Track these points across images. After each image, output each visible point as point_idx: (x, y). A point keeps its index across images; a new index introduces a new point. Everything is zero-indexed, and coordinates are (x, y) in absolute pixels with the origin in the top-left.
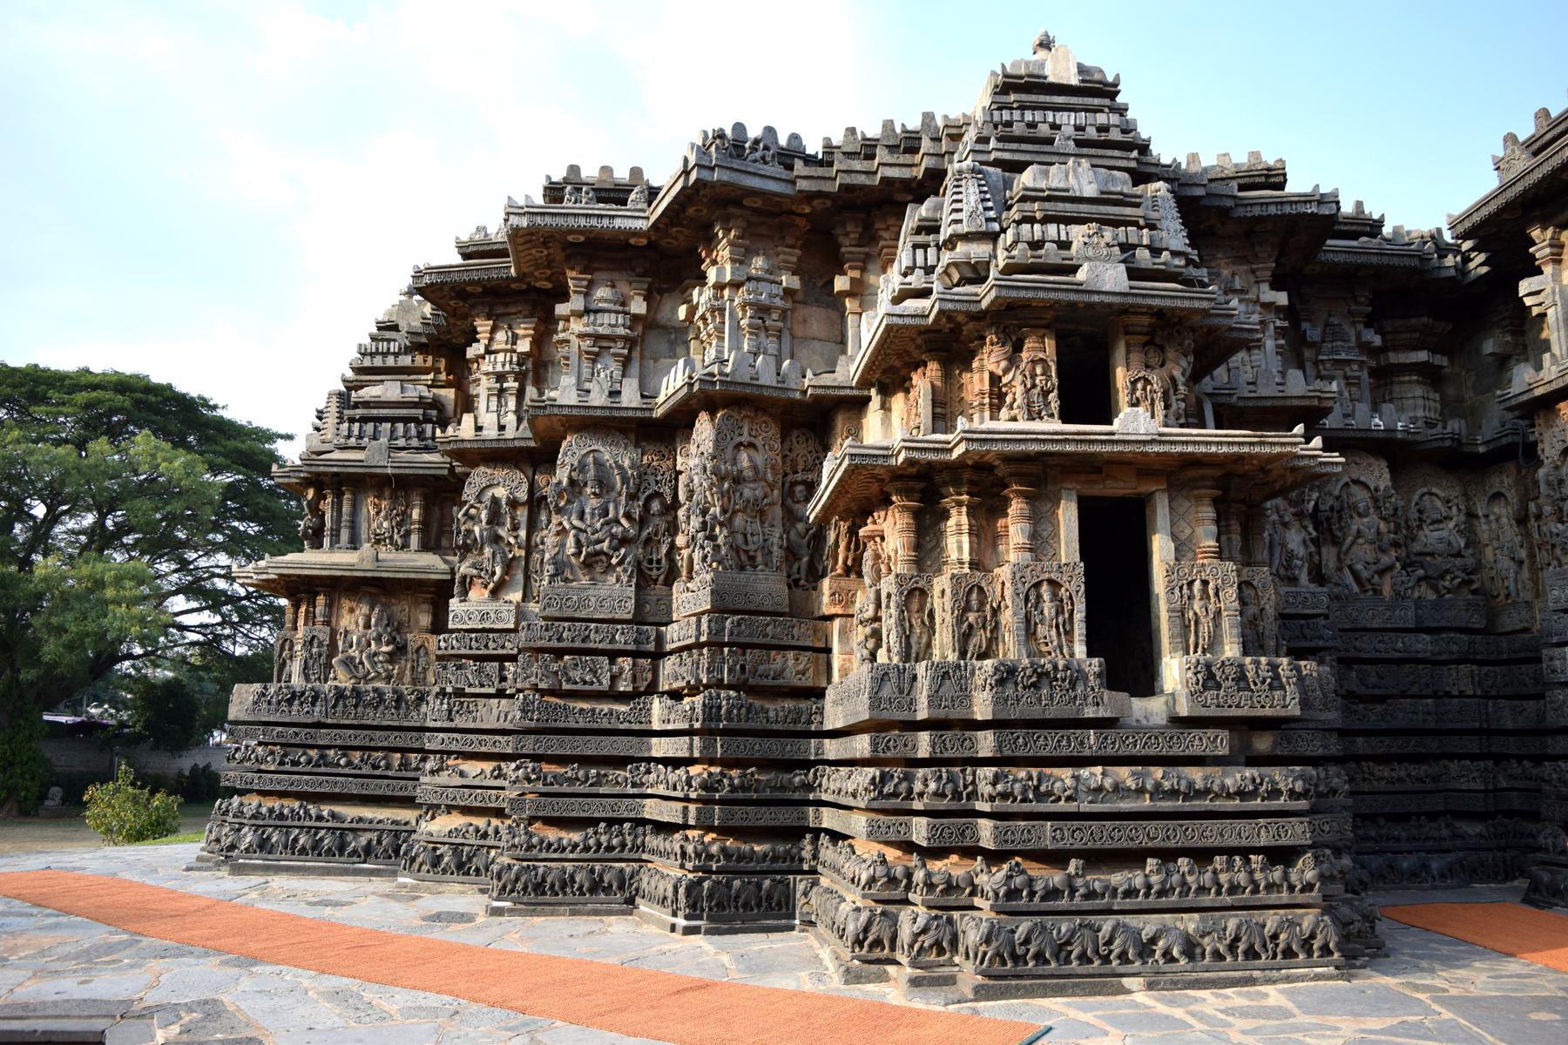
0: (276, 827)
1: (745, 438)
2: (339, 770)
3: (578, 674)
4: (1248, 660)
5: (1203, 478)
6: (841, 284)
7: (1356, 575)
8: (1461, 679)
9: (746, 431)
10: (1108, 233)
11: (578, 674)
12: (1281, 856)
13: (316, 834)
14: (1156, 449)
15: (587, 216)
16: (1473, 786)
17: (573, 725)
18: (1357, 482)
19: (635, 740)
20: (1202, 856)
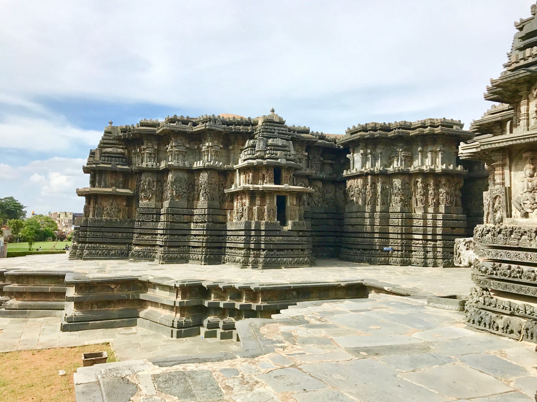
0: (93, 250)
1: (213, 176)
2: (107, 237)
3: (177, 218)
4: (300, 221)
5: (295, 193)
6: (231, 147)
7: (314, 202)
8: (331, 222)
9: (213, 175)
10: (283, 152)
11: (177, 218)
12: (302, 250)
13: (102, 251)
14: (289, 190)
15: (180, 128)
16: (332, 241)
17: (176, 228)
18: (316, 186)
19: (188, 231)
20: (292, 250)
